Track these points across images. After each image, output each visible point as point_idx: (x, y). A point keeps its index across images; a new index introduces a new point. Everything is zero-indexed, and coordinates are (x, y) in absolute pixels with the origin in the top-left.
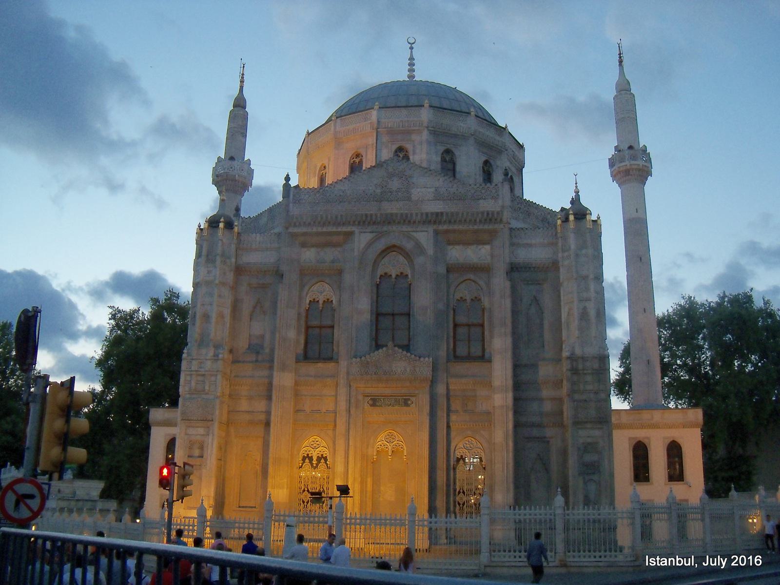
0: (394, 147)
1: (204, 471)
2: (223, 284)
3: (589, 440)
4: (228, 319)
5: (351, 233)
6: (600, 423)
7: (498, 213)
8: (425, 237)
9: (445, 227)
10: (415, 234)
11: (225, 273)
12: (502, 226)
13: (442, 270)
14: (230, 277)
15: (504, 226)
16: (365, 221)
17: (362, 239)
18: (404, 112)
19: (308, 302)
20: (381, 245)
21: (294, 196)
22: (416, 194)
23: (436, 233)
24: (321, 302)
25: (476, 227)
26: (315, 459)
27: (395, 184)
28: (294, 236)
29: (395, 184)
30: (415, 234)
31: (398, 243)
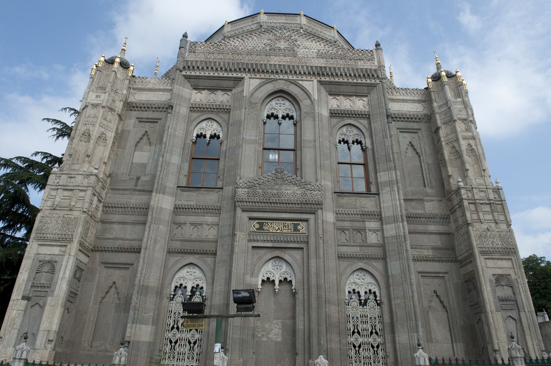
1: (49, 299)
2: (111, 109)
3: (499, 272)
4: (110, 142)
6: (508, 254)
8: (311, 85)
9: (327, 79)
10: (300, 82)
11: (114, 101)
14: (119, 106)
17: (251, 83)
19: (195, 135)
20: (270, 88)
22: (301, 52)
23: (320, 82)
25: (355, 81)
26: (189, 289)
29: (282, 45)
31: (285, 88)
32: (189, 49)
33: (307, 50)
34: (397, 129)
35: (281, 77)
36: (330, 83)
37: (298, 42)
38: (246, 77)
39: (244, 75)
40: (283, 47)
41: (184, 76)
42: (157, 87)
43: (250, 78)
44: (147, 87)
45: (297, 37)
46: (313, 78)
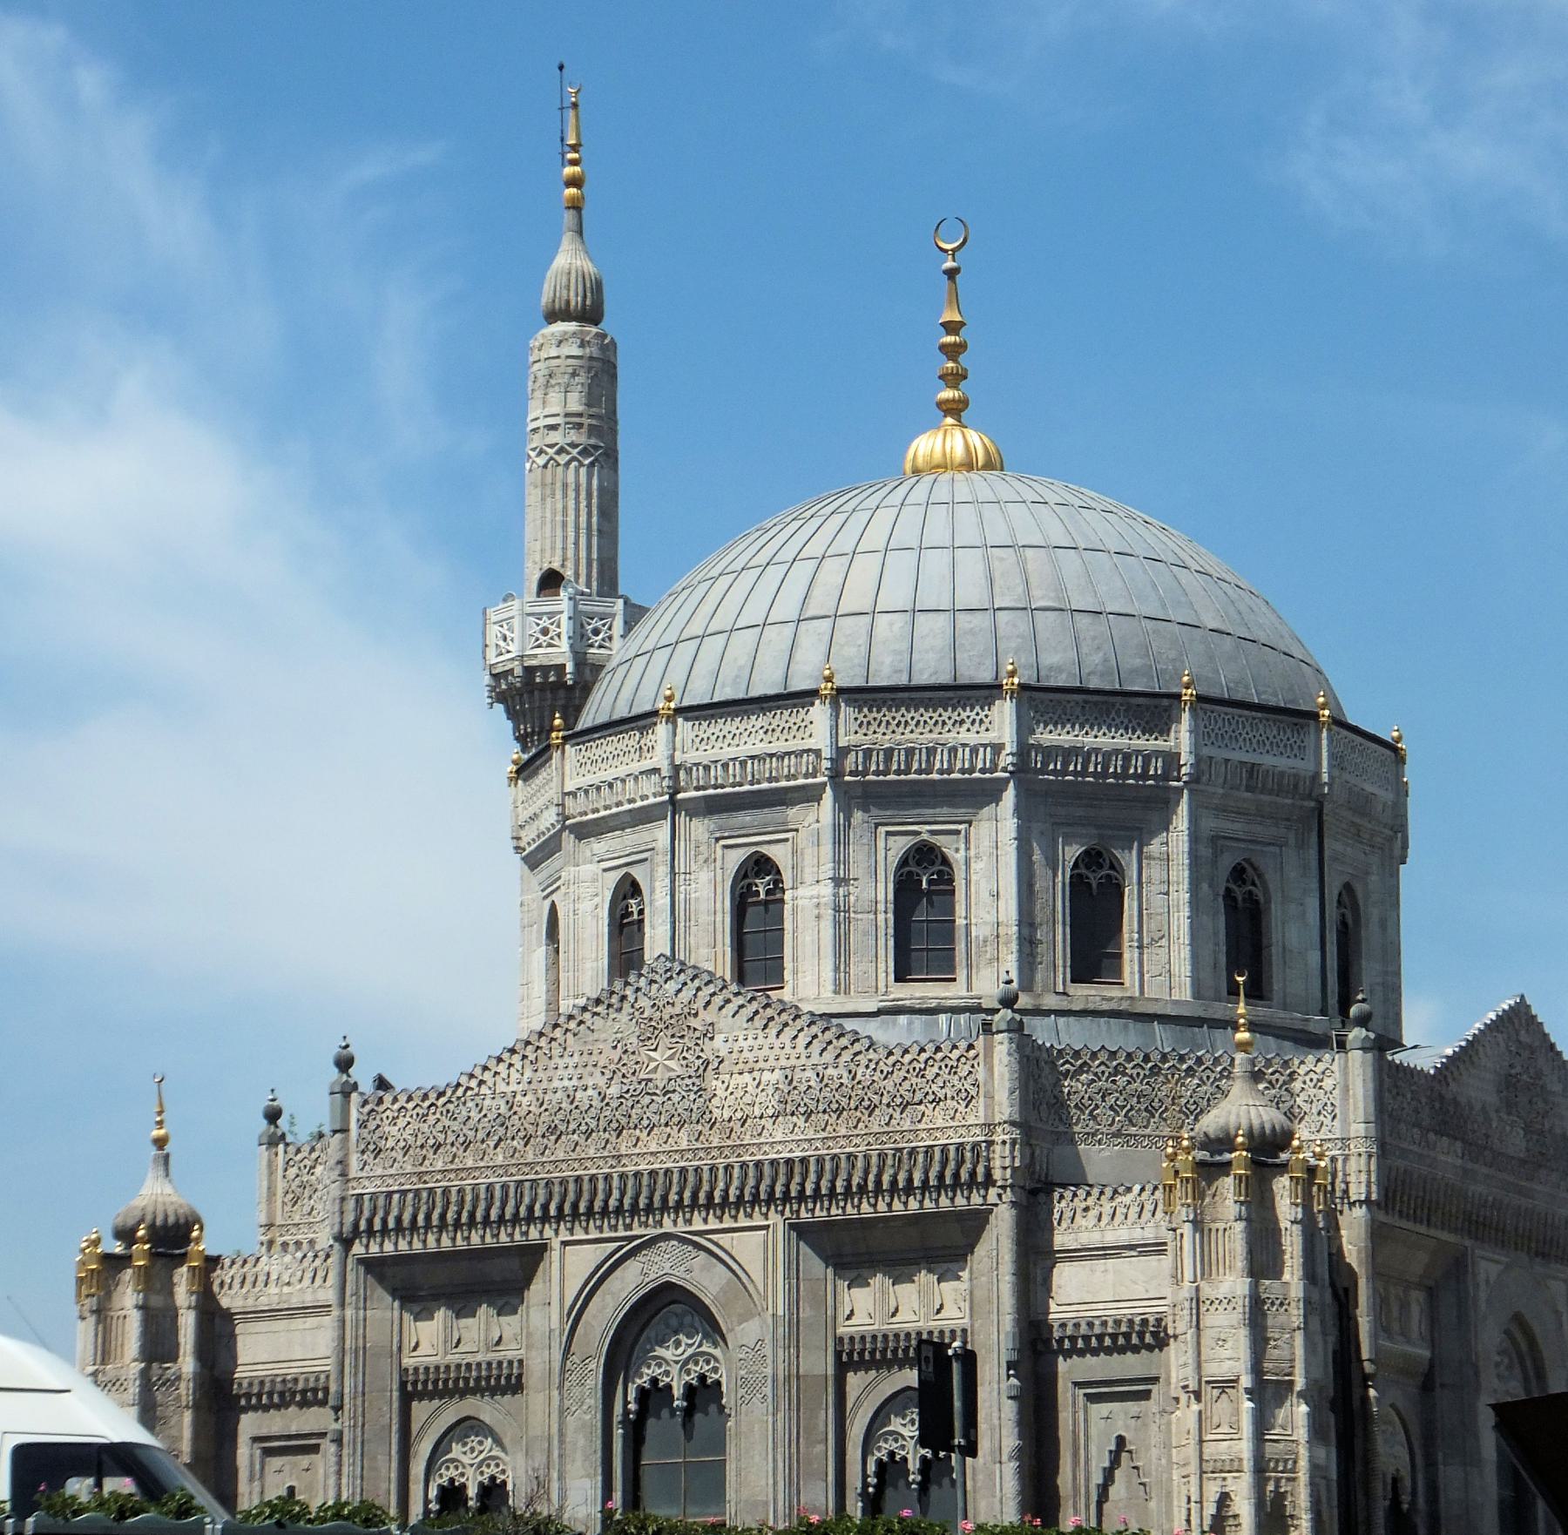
0: (736, 858)
5: (536, 1253)
7: (975, 1145)
12: (993, 1192)
13: (820, 1363)
15: (1000, 1196)
16: (579, 1206)
18: (758, 722)
20: (629, 1283)
21: (363, 1125)
23: (801, 1231)
24: (472, 1491)
27: (663, 1062)
28: (371, 1266)
29: (663, 1062)
30: (723, 1239)
31: (678, 1276)
32: (360, 1138)
33: (747, 1077)
34: (1076, 1384)
35: (668, 1226)
36: (828, 1225)
37: (719, 1038)
38: (556, 1244)
39: (548, 1232)
40: (660, 1078)
41: (361, 1261)
42: (295, 1302)
43: (565, 1244)
44: (263, 1303)
45: (707, 1016)
46: (774, 1218)
